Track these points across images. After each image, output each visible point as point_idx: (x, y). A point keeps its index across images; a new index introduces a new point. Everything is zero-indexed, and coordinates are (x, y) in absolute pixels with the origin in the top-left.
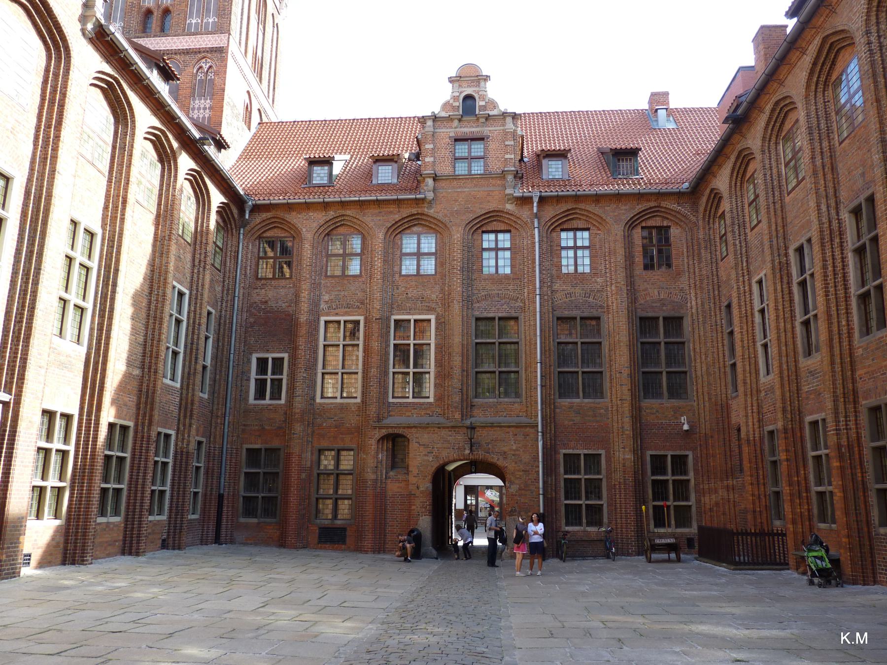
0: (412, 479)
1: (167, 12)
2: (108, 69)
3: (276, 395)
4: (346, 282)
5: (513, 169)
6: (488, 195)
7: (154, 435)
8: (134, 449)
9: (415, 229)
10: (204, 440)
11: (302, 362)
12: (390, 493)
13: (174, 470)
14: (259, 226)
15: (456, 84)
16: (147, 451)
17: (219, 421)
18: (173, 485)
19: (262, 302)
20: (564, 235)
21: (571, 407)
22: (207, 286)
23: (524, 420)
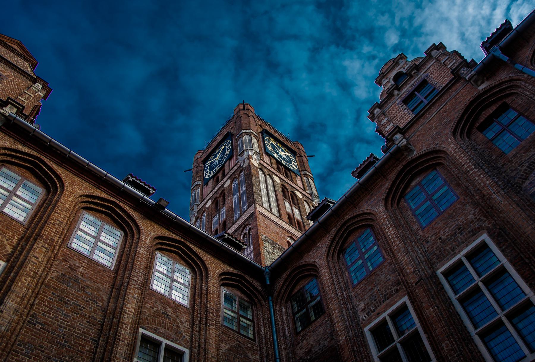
1: (225, 222)
4: (373, 277)
14: (285, 287)
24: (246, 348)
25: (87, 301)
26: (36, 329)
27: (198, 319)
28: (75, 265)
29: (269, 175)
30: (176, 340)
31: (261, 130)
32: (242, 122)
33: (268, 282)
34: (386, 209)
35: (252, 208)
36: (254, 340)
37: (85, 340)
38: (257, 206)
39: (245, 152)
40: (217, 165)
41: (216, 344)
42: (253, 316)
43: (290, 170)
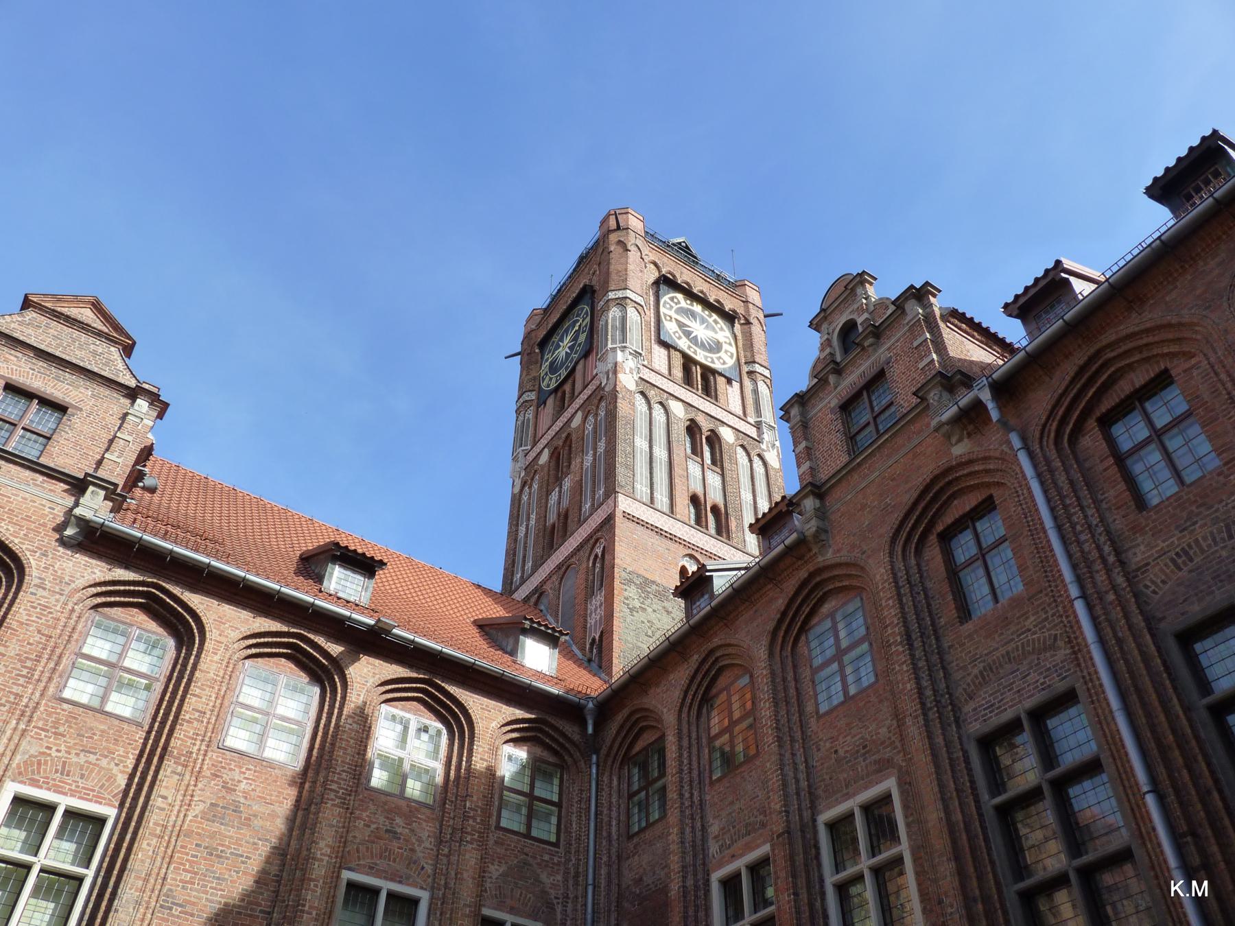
9: (826, 608)
14: (619, 739)
24: (539, 864)
25: (255, 844)
26: (173, 915)
27: (450, 830)
28: (233, 780)
29: (661, 403)
30: (408, 877)
31: (653, 275)
32: (612, 267)
33: (590, 730)
34: (771, 654)
36: (556, 845)
37: (250, 916)
38: (621, 498)
39: (610, 355)
40: (563, 364)
41: (474, 878)
42: (560, 795)
43: (714, 372)
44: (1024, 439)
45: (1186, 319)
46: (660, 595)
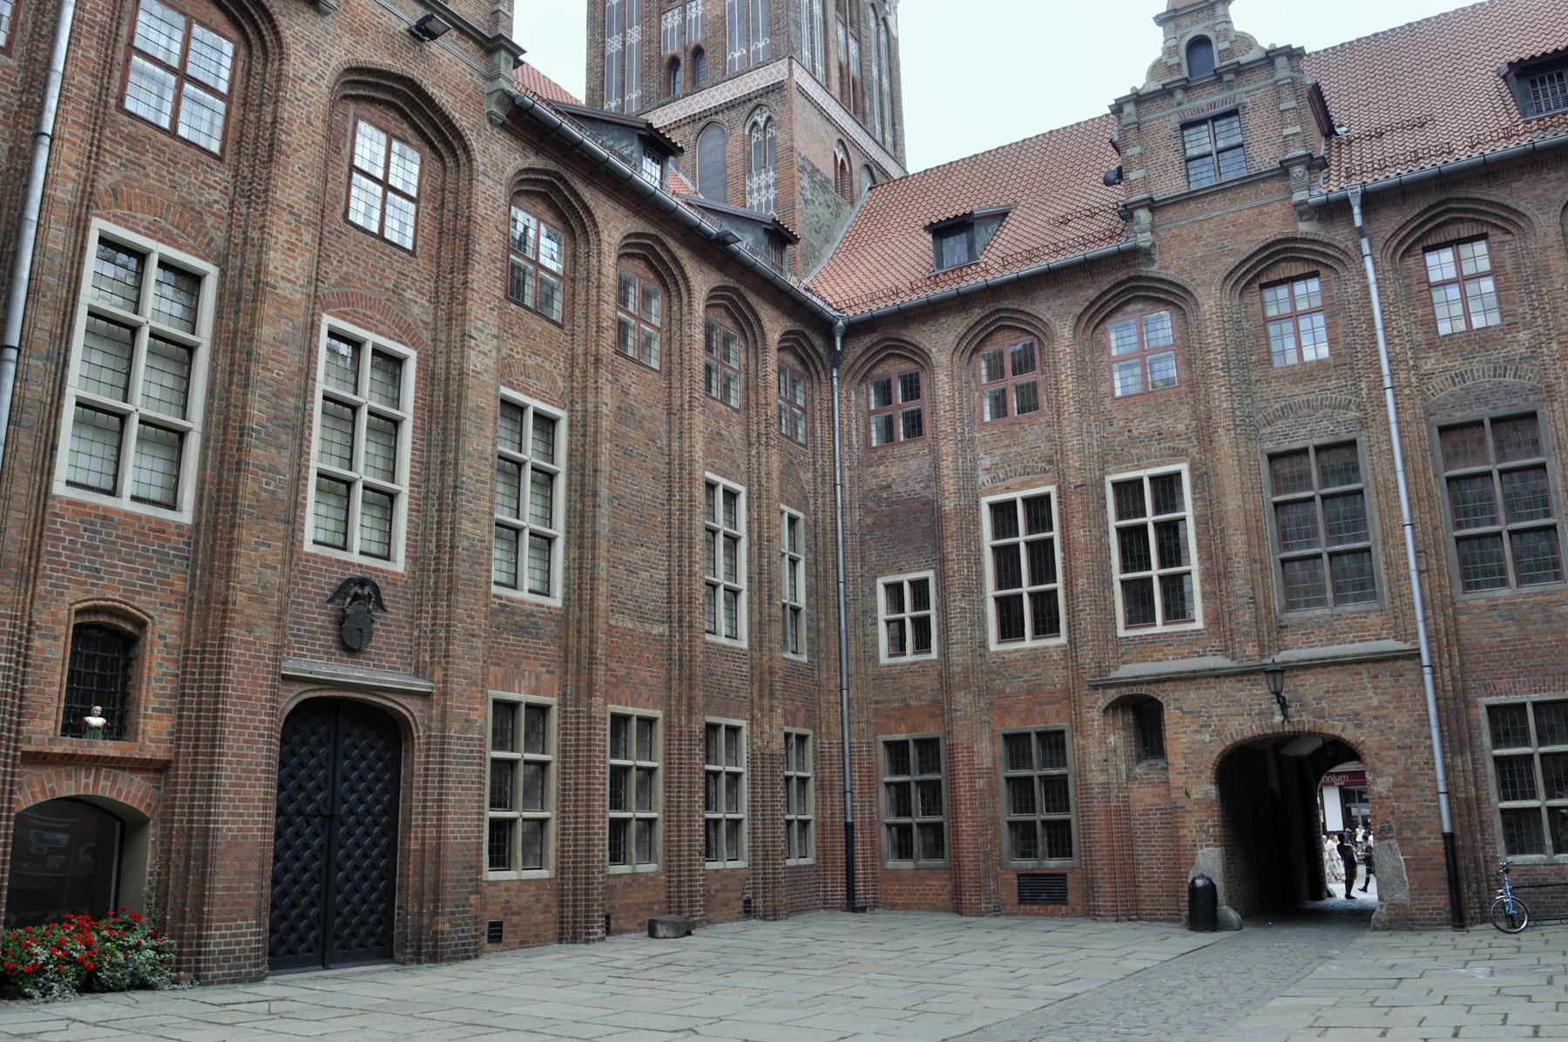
0: (1176, 780)
1: (698, 52)
2: (534, 161)
3: (923, 644)
4: (1017, 428)
5: (1302, 152)
6: (1261, 213)
7: (698, 728)
8: (668, 755)
10: (809, 732)
11: (955, 583)
12: (1138, 807)
13: (753, 786)
15: (1171, 25)
16: (691, 755)
17: (832, 698)
18: (753, 809)
19: (881, 488)
20: (1431, 259)
21: (1494, 608)
22: (775, 475)
23: (1391, 645)
35: (782, 65)
38: (795, 65)
44: (1371, 246)
45: (1521, 209)
46: (825, 190)
